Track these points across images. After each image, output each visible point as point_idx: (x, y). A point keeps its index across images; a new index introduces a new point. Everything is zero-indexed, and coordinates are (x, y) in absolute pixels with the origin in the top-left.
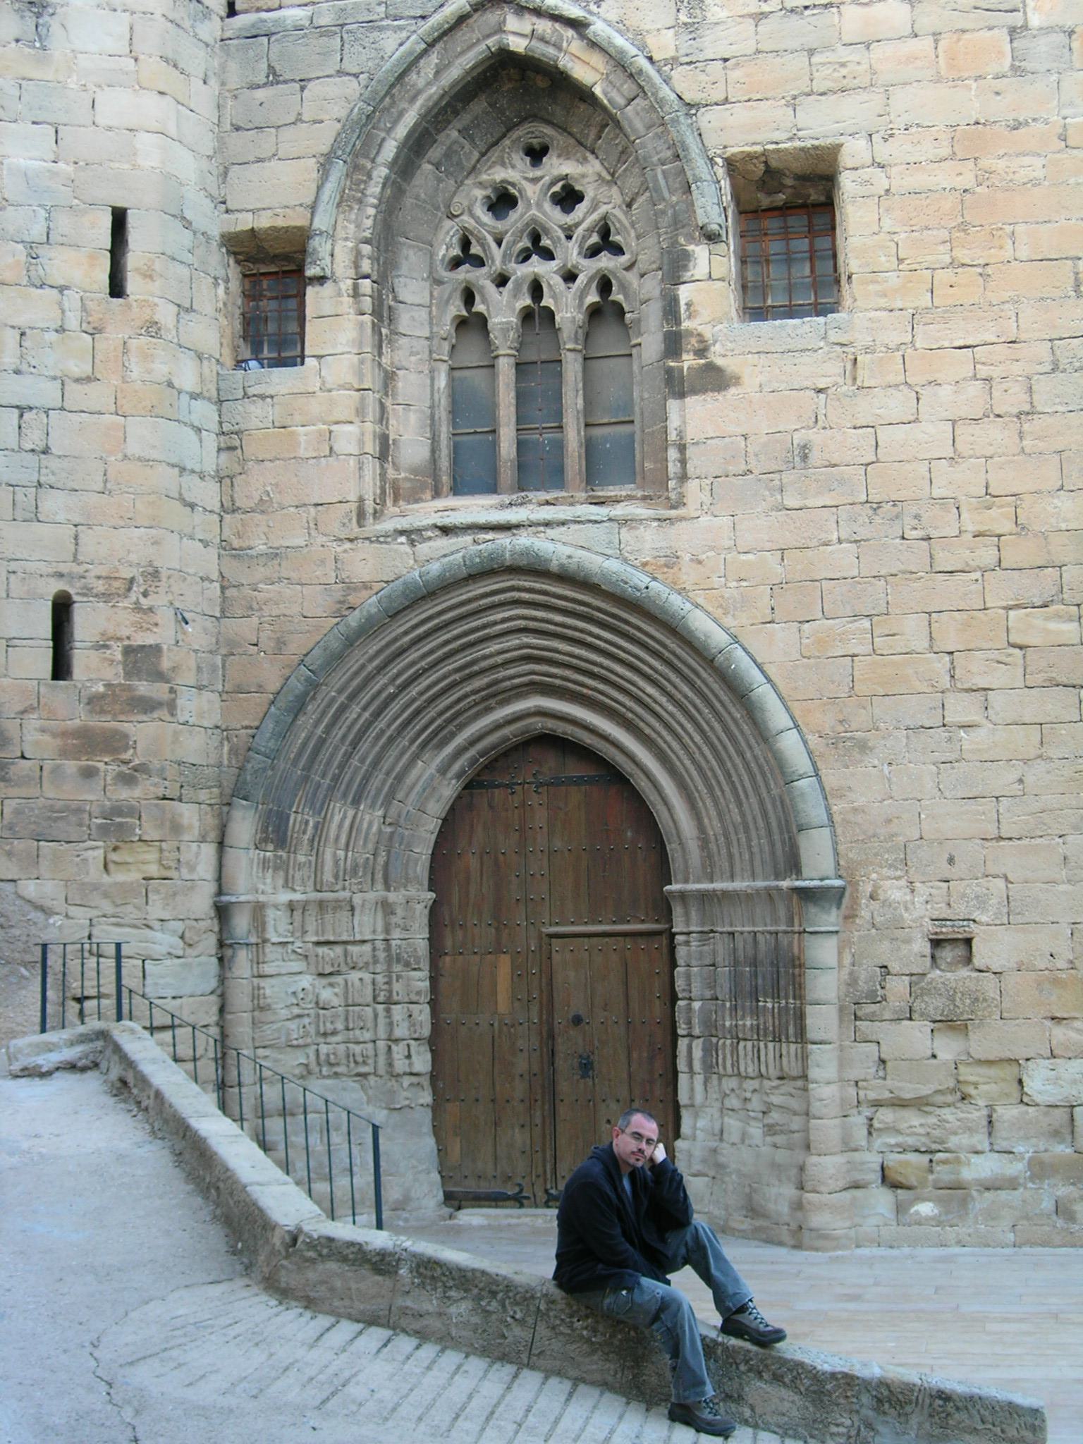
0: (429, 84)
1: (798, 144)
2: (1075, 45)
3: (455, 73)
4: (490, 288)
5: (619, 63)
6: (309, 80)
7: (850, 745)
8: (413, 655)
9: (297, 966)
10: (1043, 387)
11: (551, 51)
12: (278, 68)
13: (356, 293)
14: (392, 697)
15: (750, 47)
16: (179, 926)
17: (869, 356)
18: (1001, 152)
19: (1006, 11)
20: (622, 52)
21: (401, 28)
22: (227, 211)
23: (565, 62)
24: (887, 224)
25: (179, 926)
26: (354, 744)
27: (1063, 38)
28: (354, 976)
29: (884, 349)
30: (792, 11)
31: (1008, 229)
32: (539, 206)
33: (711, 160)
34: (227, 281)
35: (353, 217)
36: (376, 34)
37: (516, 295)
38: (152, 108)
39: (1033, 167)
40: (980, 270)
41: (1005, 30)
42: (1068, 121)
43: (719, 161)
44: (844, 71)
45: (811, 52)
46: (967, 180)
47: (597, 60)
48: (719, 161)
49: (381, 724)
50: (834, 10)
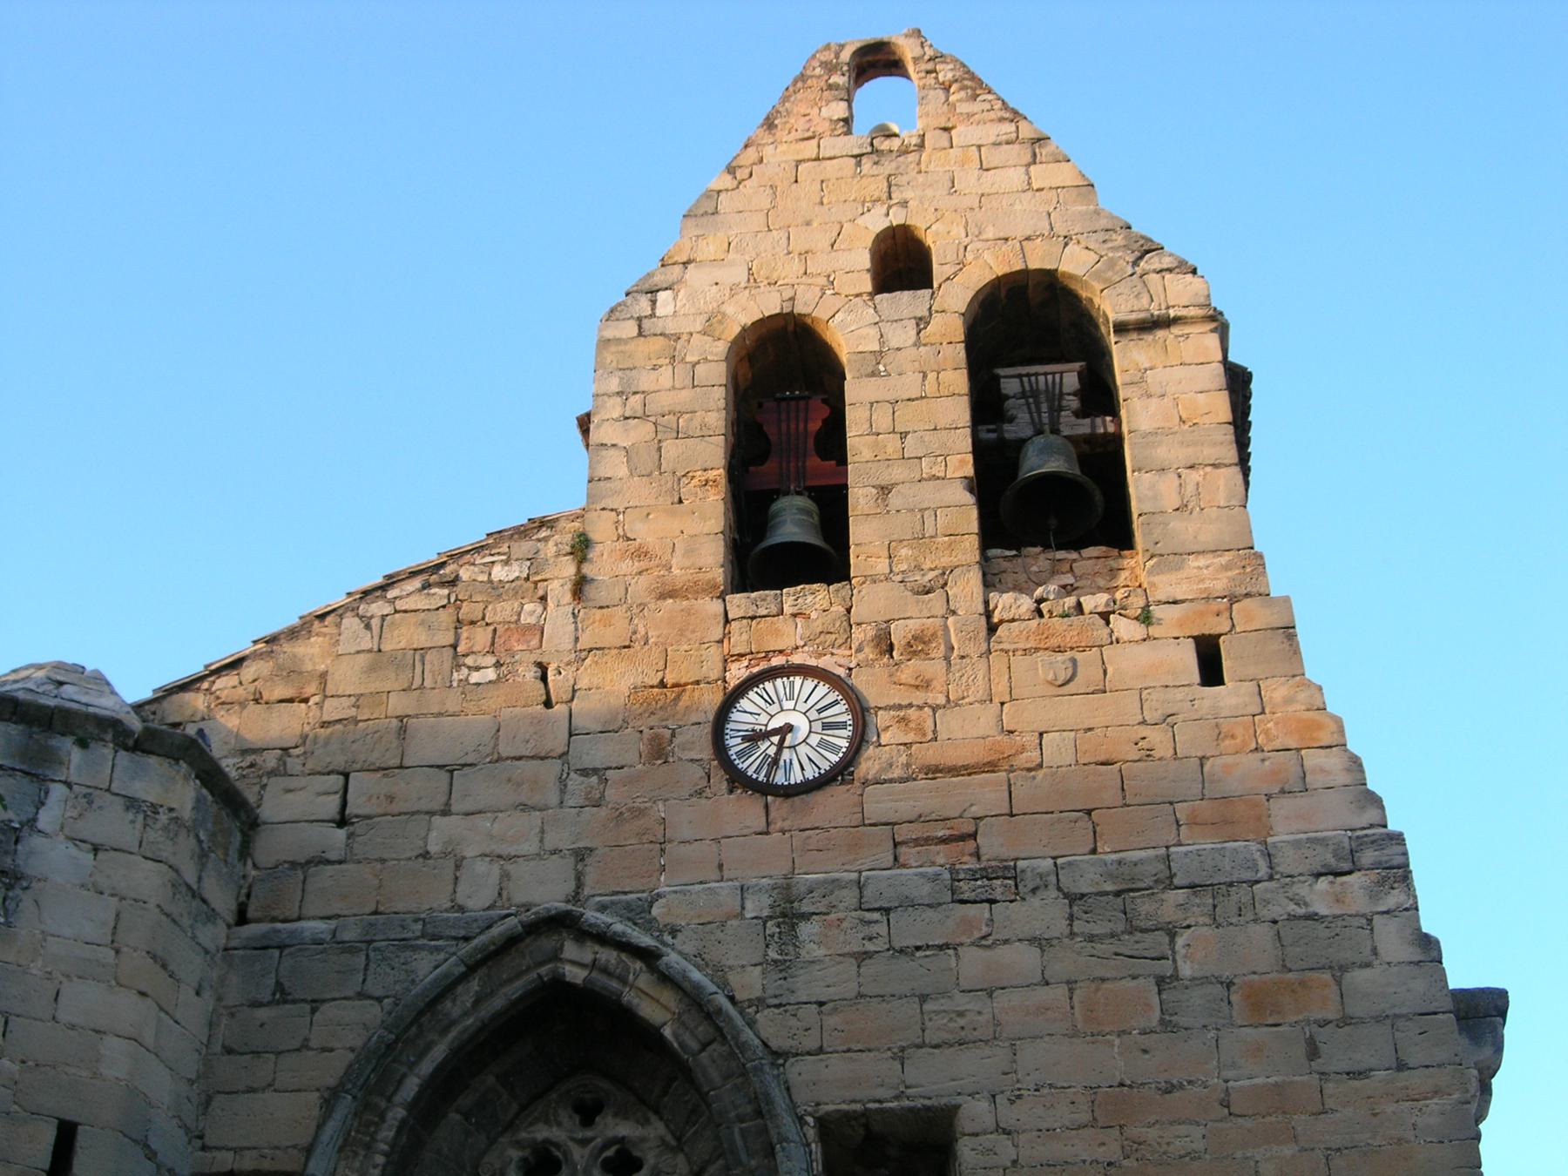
0: (466, 1014)
1: (906, 1103)
2: (1233, 998)
3: (497, 1003)
5: (694, 1000)
6: (324, 1001)
11: (615, 984)
12: (287, 984)
15: (850, 989)
18: (1152, 1119)
20: (698, 987)
21: (438, 949)
22: (204, 1148)
23: (629, 997)
27: (1218, 990)
30: (901, 951)
35: (357, 1164)
36: (408, 953)
38: (126, 1009)
39: (1191, 1138)
41: (1152, 980)
42: (1231, 1084)
43: (810, 1120)
44: (962, 1022)
45: (923, 998)
46: (1112, 1151)
47: (668, 997)
48: (810, 1120)
50: (951, 952)
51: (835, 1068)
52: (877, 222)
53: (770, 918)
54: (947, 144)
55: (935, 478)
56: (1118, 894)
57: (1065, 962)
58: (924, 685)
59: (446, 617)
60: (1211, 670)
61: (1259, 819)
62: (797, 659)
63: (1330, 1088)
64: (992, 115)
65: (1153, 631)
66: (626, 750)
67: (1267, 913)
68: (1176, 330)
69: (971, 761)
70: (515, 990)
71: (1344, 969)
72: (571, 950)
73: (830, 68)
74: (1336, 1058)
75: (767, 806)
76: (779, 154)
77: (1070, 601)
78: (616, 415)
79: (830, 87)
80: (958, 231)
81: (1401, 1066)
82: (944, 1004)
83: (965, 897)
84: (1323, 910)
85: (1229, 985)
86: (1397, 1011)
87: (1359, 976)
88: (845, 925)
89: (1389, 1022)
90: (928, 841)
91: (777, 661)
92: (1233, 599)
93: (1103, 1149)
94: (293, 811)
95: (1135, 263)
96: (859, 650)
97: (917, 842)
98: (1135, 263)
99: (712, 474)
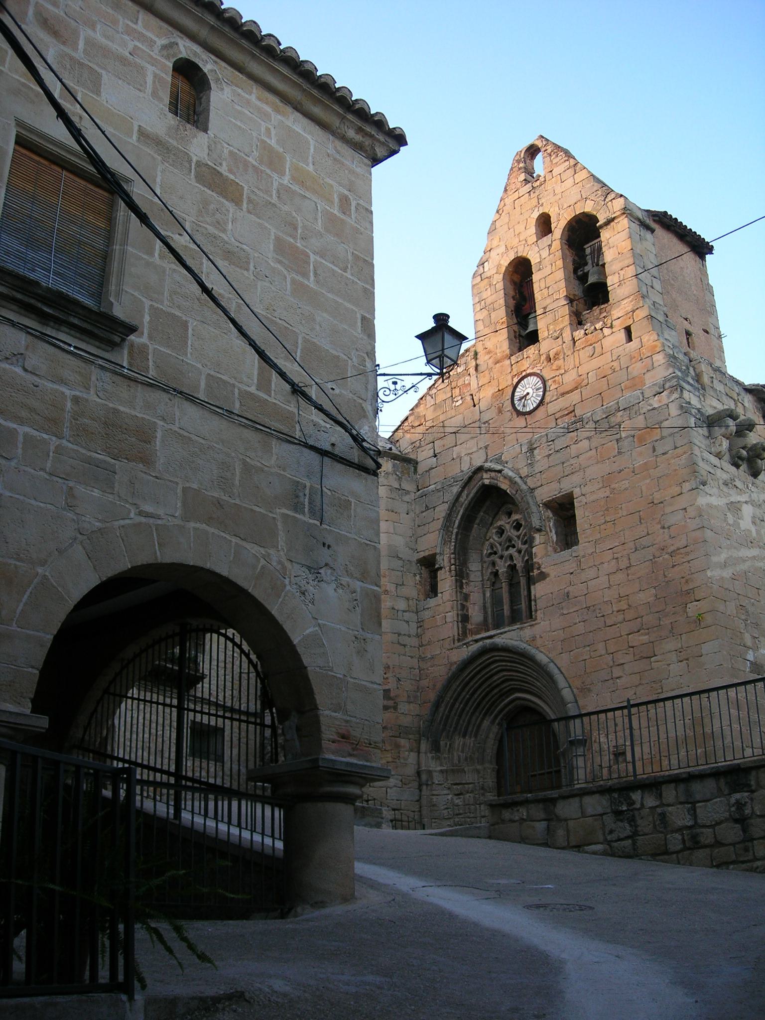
3: (471, 495)
4: (498, 561)
5: (512, 482)
7: (585, 690)
8: (472, 684)
9: (446, 792)
10: (632, 557)
13: (450, 571)
14: (469, 699)
16: (400, 778)
23: (500, 484)
24: (587, 514)
25: (400, 778)
26: (460, 716)
28: (468, 795)
34: (421, 574)
37: (505, 562)
45: (563, 463)
49: (467, 709)
51: (545, 489)
52: (536, 215)
57: (596, 442)
58: (559, 368)
59: (449, 388)
60: (629, 339)
62: (528, 372)
65: (614, 330)
67: (642, 412)
70: (474, 491)
72: (485, 475)
73: (518, 162)
74: (660, 451)
76: (508, 201)
79: (519, 169)
81: (676, 448)
82: (568, 463)
90: (564, 416)
91: (524, 374)
92: (633, 311)
94: (424, 456)
97: (561, 417)
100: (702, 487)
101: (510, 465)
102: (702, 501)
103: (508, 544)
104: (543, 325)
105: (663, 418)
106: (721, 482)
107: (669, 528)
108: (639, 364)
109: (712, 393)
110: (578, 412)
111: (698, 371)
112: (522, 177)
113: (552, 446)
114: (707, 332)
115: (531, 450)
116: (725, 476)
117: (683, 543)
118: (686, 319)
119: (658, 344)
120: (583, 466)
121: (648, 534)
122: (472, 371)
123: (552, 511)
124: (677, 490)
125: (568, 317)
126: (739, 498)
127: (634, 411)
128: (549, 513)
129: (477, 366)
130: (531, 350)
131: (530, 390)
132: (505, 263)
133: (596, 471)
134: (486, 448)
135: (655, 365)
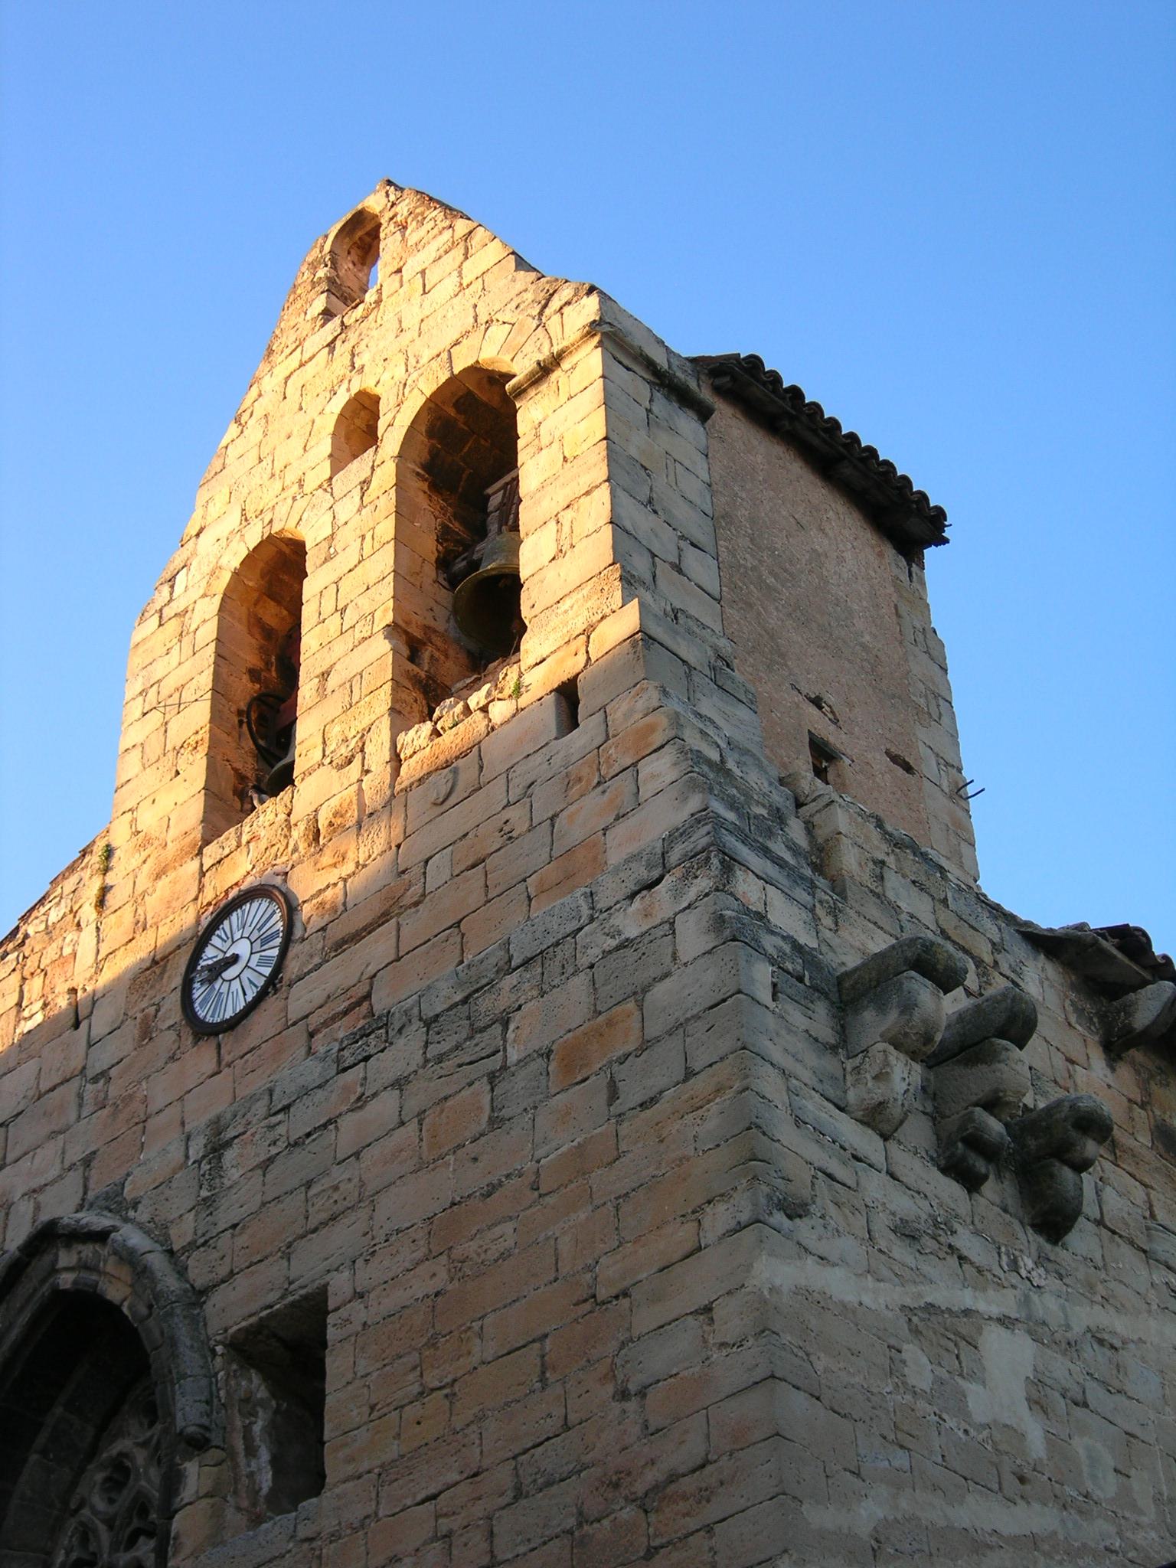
1: (291, 1298)
17: (332, 1546)
18: (474, 1231)
19: (488, 1056)
29: (349, 1531)
30: (296, 1144)
31: (476, 1325)
32: (146, 1472)
33: (213, 1352)
40: (446, 1391)
43: (219, 1349)
44: (336, 1196)
45: (308, 1185)
50: (331, 1127)
51: (242, 1284)
53: (204, 1157)
54: (397, 285)
55: (365, 639)
56: (465, 1001)
57: (418, 1097)
59: (15, 978)
61: (595, 859)
63: (625, 1129)
64: (436, 231)
66: (121, 1045)
67: (583, 961)
68: (566, 365)
69: (369, 920)
71: (645, 990)
74: (632, 1094)
75: (219, 1047)
77: (460, 707)
78: (138, 714)
80: (400, 373)
81: (690, 1074)
82: (326, 1183)
83: (346, 1065)
84: (632, 932)
85: (548, 1054)
86: (688, 1015)
87: (660, 990)
88: (257, 1136)
89: (681, 1030)
90: (334, 1019)
93: (435, 1279)
95: (541, 313)
96: (295, 850)
98: (541, 313)
99: (199, 737)
100: (779, 1218)
101: (143, 1214)
102: (777, 1272)
103: (136, 1523)
104: (312, 729)
105: (655, 971)
106: (881, 1222)
107: (642, 1393)
108: (594, 801)
109: (873, 910)
110: (381, 1002)
111: (821, 834)
112: (320, 303)
113: (281, 1130)
114: (908, 768)
115: (216, 1149)
116: (904, 1204)
117: (694, 1448)
118: (817, 702)
119: (661, 719)
120: (370, 1188)
121: (567, 1427)
122: (88, 913)
123: (267, 1377)
124: (683, 1235)
125: (388, 687)
126: (967, 1298)
127: (554, 967)
128: (255, 1385)
129: (105, 890)
130: (268, 813)
131: (242, 948)
132: (233, 559)
133: (407, 1202)
134: (87, 1162)
135: (644, 794)
